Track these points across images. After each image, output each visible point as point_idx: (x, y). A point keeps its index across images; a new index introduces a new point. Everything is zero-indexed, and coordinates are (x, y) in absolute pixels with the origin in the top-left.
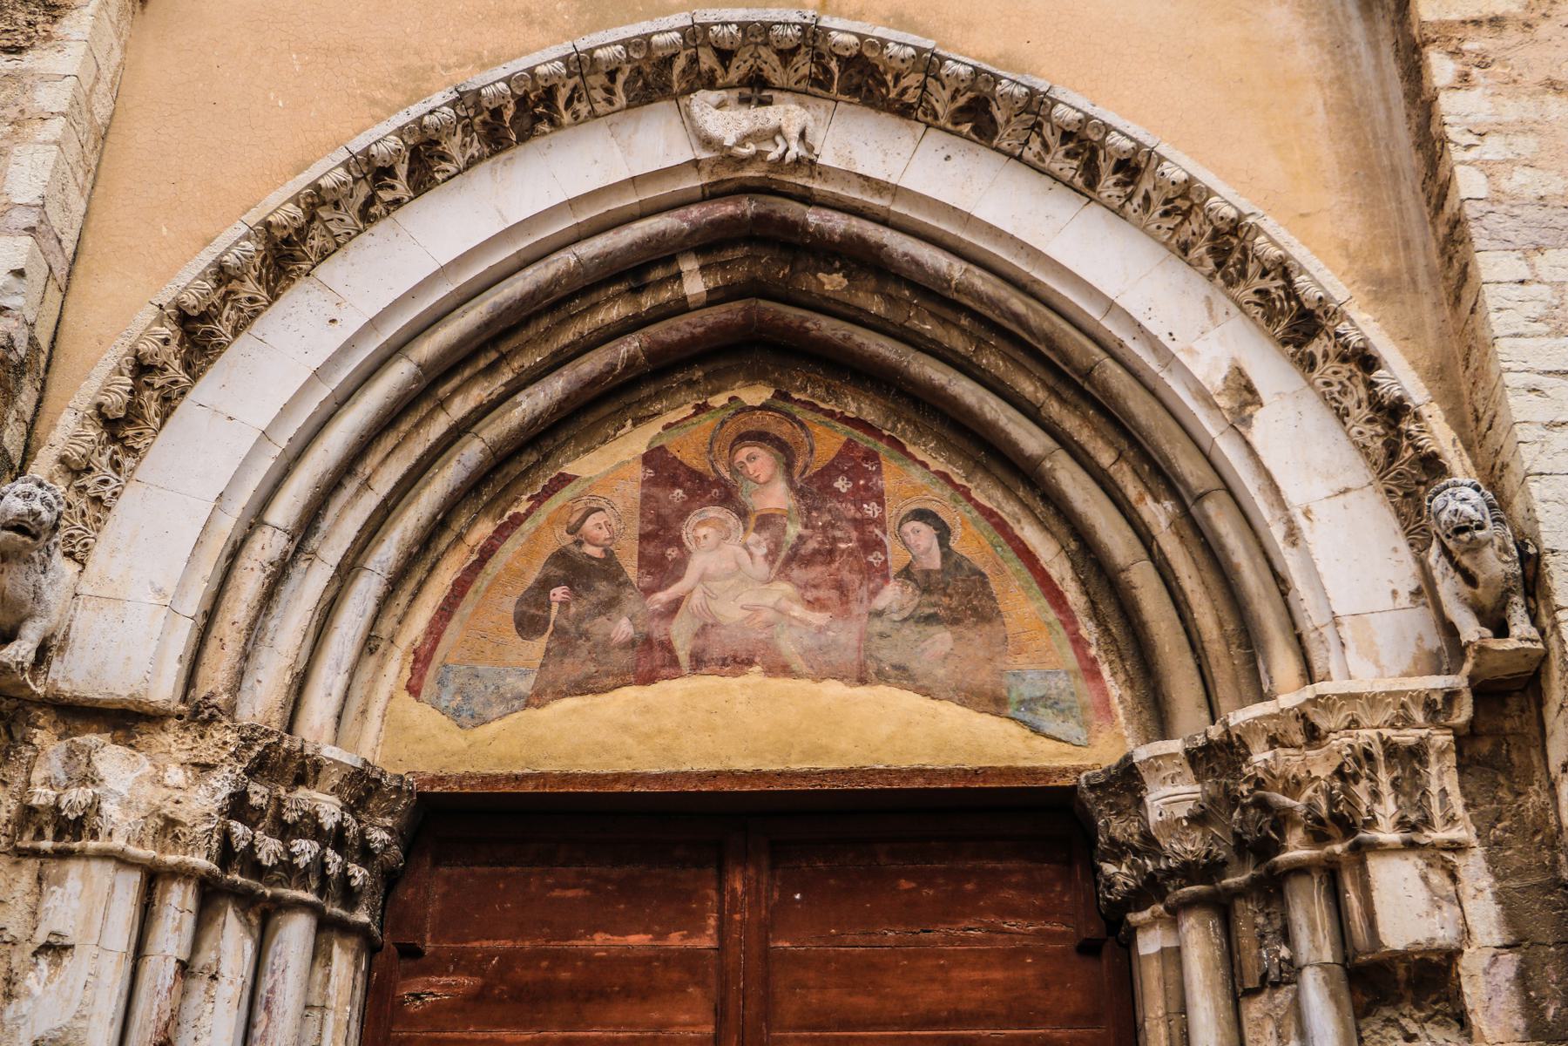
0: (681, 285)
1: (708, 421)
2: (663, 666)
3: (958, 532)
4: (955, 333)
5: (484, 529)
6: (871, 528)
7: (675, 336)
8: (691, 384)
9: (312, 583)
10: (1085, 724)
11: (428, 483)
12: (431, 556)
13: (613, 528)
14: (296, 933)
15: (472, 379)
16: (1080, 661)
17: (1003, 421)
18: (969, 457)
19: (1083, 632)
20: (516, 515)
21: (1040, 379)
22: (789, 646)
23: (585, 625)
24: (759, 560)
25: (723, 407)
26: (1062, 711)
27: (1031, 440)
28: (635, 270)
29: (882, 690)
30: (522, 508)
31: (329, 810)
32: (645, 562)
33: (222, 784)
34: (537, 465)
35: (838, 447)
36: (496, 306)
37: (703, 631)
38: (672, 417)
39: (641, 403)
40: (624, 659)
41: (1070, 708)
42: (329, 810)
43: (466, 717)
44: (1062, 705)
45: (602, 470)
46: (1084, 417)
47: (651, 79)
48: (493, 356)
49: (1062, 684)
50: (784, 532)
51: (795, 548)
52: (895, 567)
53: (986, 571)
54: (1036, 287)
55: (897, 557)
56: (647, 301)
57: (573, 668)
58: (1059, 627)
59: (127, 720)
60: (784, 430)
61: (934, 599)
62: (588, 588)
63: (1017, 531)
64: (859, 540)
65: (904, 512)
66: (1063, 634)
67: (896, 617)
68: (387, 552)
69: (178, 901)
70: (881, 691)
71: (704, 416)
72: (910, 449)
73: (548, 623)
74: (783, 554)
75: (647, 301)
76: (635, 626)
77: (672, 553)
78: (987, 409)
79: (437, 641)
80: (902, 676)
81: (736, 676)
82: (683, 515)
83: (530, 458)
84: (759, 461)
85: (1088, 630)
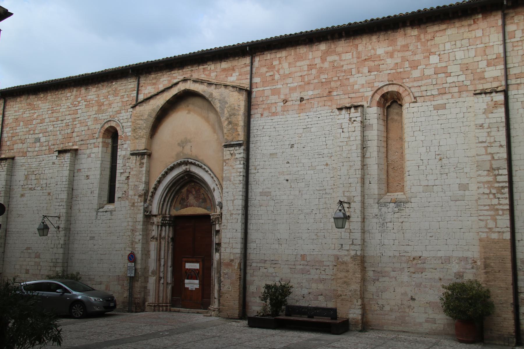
9: (166, 203)
14: (167, 227)
22: (195, 205)
28: (182, 178)
31: (168, 219)
33: (161, 219)
43: (177, 211)
59: (155, 216)
68: (170, 200)
69: (160, 227)
80: (201, 207)
84: (193, 190)
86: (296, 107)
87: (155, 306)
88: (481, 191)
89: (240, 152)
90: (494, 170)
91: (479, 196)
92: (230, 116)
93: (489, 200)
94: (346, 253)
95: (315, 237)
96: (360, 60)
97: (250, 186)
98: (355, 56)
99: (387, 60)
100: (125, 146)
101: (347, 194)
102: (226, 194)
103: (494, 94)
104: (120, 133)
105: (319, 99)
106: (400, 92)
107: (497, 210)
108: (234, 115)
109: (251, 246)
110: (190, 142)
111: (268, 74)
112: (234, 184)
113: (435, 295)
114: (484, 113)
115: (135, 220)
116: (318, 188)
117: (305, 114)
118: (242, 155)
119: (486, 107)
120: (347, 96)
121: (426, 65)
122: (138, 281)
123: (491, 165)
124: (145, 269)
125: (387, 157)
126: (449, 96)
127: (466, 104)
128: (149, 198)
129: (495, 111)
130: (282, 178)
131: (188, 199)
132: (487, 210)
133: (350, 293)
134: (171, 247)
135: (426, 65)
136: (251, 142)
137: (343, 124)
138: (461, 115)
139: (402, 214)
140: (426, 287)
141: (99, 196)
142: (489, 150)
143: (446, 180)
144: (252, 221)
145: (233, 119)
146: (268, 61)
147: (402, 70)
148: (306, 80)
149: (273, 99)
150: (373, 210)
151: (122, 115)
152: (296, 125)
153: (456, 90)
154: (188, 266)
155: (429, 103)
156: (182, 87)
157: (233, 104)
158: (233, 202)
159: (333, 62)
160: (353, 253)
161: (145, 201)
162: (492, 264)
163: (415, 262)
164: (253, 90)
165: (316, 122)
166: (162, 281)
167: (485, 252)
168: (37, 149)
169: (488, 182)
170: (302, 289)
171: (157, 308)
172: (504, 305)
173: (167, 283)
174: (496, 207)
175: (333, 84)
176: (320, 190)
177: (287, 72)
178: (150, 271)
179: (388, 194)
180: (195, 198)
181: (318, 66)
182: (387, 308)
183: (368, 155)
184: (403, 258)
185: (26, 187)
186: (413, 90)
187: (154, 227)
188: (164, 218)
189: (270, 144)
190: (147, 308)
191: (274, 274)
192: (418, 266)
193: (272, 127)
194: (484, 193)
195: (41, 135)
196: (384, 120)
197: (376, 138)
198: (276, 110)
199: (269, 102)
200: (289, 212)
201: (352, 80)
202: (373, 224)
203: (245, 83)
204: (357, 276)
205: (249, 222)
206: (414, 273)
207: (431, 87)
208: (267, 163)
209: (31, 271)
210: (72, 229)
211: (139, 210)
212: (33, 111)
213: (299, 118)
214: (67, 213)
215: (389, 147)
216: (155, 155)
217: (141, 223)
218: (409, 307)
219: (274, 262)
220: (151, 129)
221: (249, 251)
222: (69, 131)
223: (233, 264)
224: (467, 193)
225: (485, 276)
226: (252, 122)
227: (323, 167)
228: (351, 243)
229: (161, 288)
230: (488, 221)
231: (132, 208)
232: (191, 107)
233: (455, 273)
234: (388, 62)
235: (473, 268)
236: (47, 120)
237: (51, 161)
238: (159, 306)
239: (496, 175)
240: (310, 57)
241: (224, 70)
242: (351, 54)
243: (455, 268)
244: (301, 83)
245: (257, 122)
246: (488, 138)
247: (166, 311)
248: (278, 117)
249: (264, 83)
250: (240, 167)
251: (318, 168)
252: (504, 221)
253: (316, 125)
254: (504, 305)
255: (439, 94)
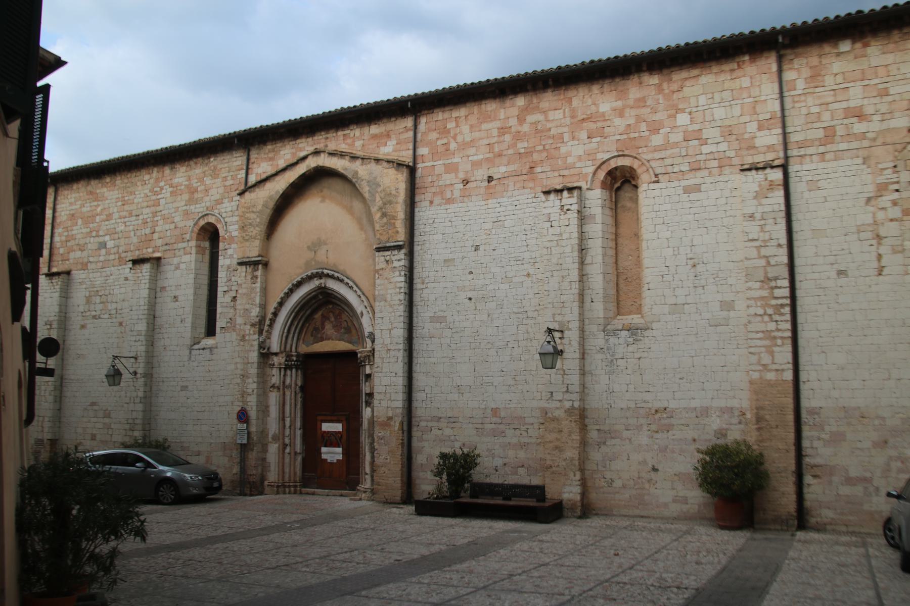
9: (291, 336)
14: (294, 370)
28: (314, 297)
31: (295, 359)
42: (295, 359)
47: (310, 278)
59: (276, 354)
69: (283, 370)
84: (331, 315)
86: (482, 191)
87: (278, 487)
88: (752, 311)
89: (399, 259)
90: (770, 280)
91: (750, 318)
92: (385, 204)
93: (763, 325)
94: (558, 404)
95: (512, 382)
96: (576, 120)
97: (415, 308)
98: (567, 114)
99: (615, 120)
100: (230, 252)
101: (558, 318)
102: (380, 321)
103: (768, 171)
104: (222, 233)
105: (516, 178)
106: (635, 167)
107: (775, 338)
108: (390, 202)
109: (418, 396)
110: (326, 244)
111: (439, 143)
112: (391, 306)
113: (687, 463)
114: (755, 198)
115: (246, 361)
116: (516, 310)
117: (495, 201)
118: (402, 263)
119: (757, 189)
120: (556, 174)
121: (672, 128)
122: (252, 450)
123: (766, 273)
124: (263, 433)
125: (616, 263)
126: (705, 173)
127: (729, 185)
128: (266, 328)
129: (770, 195)
130: (463, 296)
131: (323, 328)
132: (760, 339)
133: (564, 463)
134: (299, 400)
135: (672, 128)
136: (415, 243)
137: (552, 215)
138: (723, 201)
139: (639, 346)
140: (673, 452)
141: (192, 327)
142: (764, 252)
143: (702, 296)
144: (418, 361)
145: (389, 209)
146: (439, 123)
147: (636, 135)
148: (496, 150)
149: (448, 178)
150: (597, 340)
151: (224, 205)
152: (483, 216)
153: (715, 164)
154: (326, 427)
155: (676, 184)
156: (312, 163)
157: (389, 187)
158: (390, 333)
159: (535, 123)
160: (568, 405)
161: (261, 332)
162: (767, 417)
163: (658, 416)
164: (418, 166)
165: (512, 213)
166: (288, 450)
167: (757, 400)
168: (102, 258)
169: (762, 298)
170: (493, 458)
171: (281, 489)
172: (783, 474)
173: (296, 453)
174: (773, 334)
175: (536, 156)
176: (519, 313)
177: (468, 139)
178: (270, 436)
179: (619, 317)
180: (334, 327)
181: (513, 130)
182: (618, 483)
183: (588, 260)
184: (641, 411)
185: (88, 314)
186: (653, 164)
187: (275, 371)
188: (289, 357)
189: (443, 245)
190: (267, 489)
191: (452, 438)
192: (663, 422)
193: (447, 220)
194: (756, 314)
195: (107, 238)
196: (612, 209)
197: (600, 234)
198: (453, 194)
199: (441, 183)
200: (473, 345)
201: (563, 150)
202: (597, 361)
203: (406, 156)
204: (575, 437)
205: (415, 361)
206: (657, 432)
207: (680, 160)
208: (439, 273)
209: (98, 437)
210: (155, 376)
211: (252, 345)
212: (96, 203)
213: (486, 207)
214: (147, 352)
215: (620, 248)
216: (274, 264)
217: (256, 365)
218: (650, 481)
219: (452, 420)
220: (268, 227)
221: (415, 404)
222: (148, 231)
223: (392, 423)
224: (732, 314)
225: (757, 433)
226: (416, 214)
227: (523, 279)
228: (565, 389)
229: (287, 460)
230: (762, 355)
231: (242, 343)
232: (326, 192)
233: (715, 431)
234: (616, 124)
235: (740, 423)
236: (116, 216)
237: (123, 276)
238: (285, 487)
239: (772, 288)
240: (502, 117)
241: (375, 137)
242: (561, 111)
243: (715, 423)
244: (488, 156)
245: (424, 213)
246: (761, 234)
247: (295, 493)
248: (456, 205)
249: (434, 154)
250: (400, 280)
251: (514, 280)
252: (784, 354)
253: (512, 217)
254: (783, 474)
255: (692, 170)
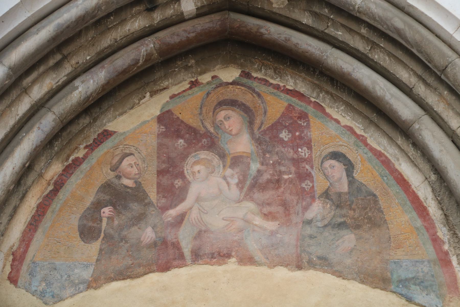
0: (180, 5)
1: (198, 93)
2: (175, 259)
3: (358, 167)
4: (357, 38)
5: (56, 168)
6: (304, 164)
7: (176, 40)
8: (187, 68)
10: (441, 296)
11: (19, 143)
12: (22, 189)
13: (138, 168)
15: (46, 72)
16: (437, 254)
17: (388, 97)
18: (366, 117)
19: (440, 234)
20: (77, 159)
21: (412, 70)
22: (253, 245)
23: (124, 233)
24: (234, 187)
25: (208, 83)
26: (426, 287)
27: (405, 108)
29: (312, 273)
30: (80, 154)
32: (163, 190)
34: (89, 125)
35: (282, 110)
36: (59, 24)
37: (199, 235)
38: (175, 90)
39: (155, 82)
40: (149, 255)
41: (431, 286)
44: (426, 284)
45: (132, 127)
46: (440, 95)
48: (58, 57)
49: (426, 269)
50: (249, 168)
51: (256, 179)
52: (319, 190)
53: (377, 193)
54: (411, 10)
55: (320, 184)
56: (158, 17)
57: (119, 261)
58: (424, 231)
60: (247, 98)
61: (344, 211)
62: (125, 207)
63: (397, 166)
64: (296, 173)
65: (324, 154)
66: (427, 235)
67: (320, 224)
70: (312, 274)
71: (196, 89)
72: (328, 110)
73: (100, 231)
74: (248, 183)
75: (158, 17)
76: (156, 233)
77: (178, 183)
78: (377, 88)
79: (28, 246)
80: (324, 264)
81: (220, 265)
82: (184, 157)
83: (85, 121)
84: (232, 120)
85: (443, 232)
180: (252, 187)
